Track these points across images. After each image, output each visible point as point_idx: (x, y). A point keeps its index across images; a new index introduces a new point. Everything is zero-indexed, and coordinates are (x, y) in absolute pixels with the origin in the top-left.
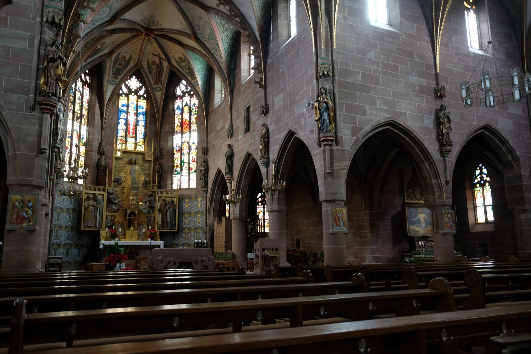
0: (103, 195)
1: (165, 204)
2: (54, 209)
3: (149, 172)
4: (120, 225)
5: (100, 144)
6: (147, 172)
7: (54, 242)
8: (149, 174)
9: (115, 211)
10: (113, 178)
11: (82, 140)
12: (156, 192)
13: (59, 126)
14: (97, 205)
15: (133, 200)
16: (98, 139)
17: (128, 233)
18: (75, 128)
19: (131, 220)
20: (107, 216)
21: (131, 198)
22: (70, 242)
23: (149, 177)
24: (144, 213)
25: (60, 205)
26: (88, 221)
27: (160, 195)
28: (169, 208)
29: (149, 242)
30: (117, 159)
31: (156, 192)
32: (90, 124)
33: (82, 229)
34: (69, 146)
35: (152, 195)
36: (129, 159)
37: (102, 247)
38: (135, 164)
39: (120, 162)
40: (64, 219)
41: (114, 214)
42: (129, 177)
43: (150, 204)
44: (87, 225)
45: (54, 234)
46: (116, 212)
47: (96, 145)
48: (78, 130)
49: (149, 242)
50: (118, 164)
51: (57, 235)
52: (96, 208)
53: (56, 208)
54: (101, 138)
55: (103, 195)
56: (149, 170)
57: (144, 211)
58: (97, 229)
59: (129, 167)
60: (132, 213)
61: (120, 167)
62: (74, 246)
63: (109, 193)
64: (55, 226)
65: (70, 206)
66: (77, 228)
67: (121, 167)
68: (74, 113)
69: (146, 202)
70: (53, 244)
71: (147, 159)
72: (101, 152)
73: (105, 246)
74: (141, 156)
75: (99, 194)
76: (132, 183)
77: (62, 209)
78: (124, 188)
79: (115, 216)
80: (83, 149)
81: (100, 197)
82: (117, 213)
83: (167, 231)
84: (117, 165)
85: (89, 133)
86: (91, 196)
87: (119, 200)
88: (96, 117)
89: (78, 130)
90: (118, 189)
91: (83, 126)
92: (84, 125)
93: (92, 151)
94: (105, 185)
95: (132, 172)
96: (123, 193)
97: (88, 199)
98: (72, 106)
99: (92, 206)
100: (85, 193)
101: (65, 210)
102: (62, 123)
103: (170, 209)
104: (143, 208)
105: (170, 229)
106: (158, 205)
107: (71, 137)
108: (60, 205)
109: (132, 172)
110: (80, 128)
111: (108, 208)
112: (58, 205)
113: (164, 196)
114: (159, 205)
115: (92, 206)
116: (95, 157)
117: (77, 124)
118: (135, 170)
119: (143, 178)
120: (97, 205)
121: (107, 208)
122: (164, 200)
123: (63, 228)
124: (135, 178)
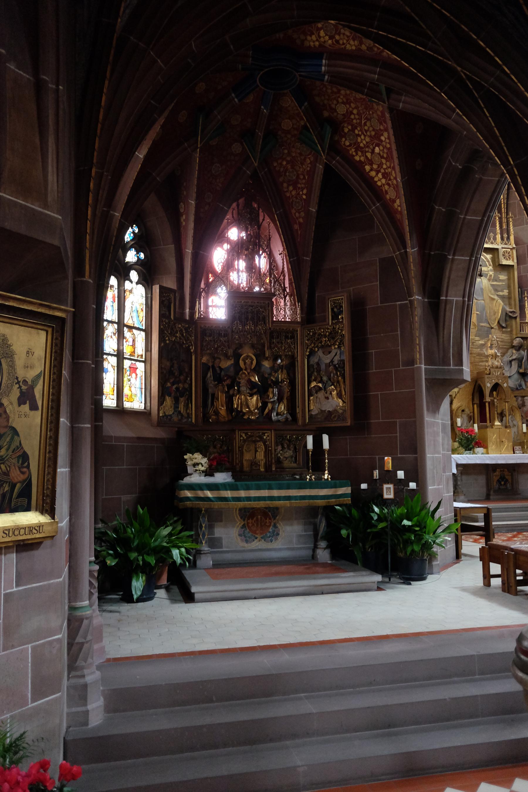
4: (465, 416)
6: (506, 292)
8: (509, 298)
17: (492, 435)
23: (510, 304)
43: (520, 366)
71: (505, 262)
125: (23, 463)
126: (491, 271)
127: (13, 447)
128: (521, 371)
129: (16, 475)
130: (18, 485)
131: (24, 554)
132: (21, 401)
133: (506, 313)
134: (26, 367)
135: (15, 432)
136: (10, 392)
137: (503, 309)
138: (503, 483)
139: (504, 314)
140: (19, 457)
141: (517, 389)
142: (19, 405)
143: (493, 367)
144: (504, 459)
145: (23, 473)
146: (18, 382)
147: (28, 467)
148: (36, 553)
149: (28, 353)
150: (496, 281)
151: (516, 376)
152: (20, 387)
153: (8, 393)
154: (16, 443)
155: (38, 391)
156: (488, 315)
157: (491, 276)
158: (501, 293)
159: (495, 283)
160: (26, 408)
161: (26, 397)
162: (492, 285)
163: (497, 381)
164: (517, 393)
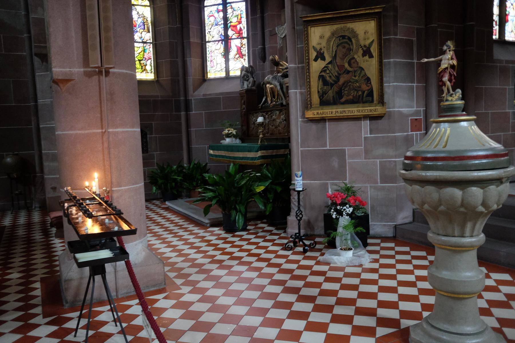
125: (368, 82)
127: (361, 75)
129: (364, 87)
130: (366, 92)
131: (373, 121)
132: (364, 55)
134: (365, 39)
135: (362, 69)
136: (357, 52)
140: (365, 79)
142: (363, 57)
145: (368, 86)
146: (361, 47)
147: (370, 83)
148: (380, 121)
149: (365, 33)
152: (363, 49)
153: (357, 52)
154: (363, 74)
160: (367, 57)
161: (367, 52)
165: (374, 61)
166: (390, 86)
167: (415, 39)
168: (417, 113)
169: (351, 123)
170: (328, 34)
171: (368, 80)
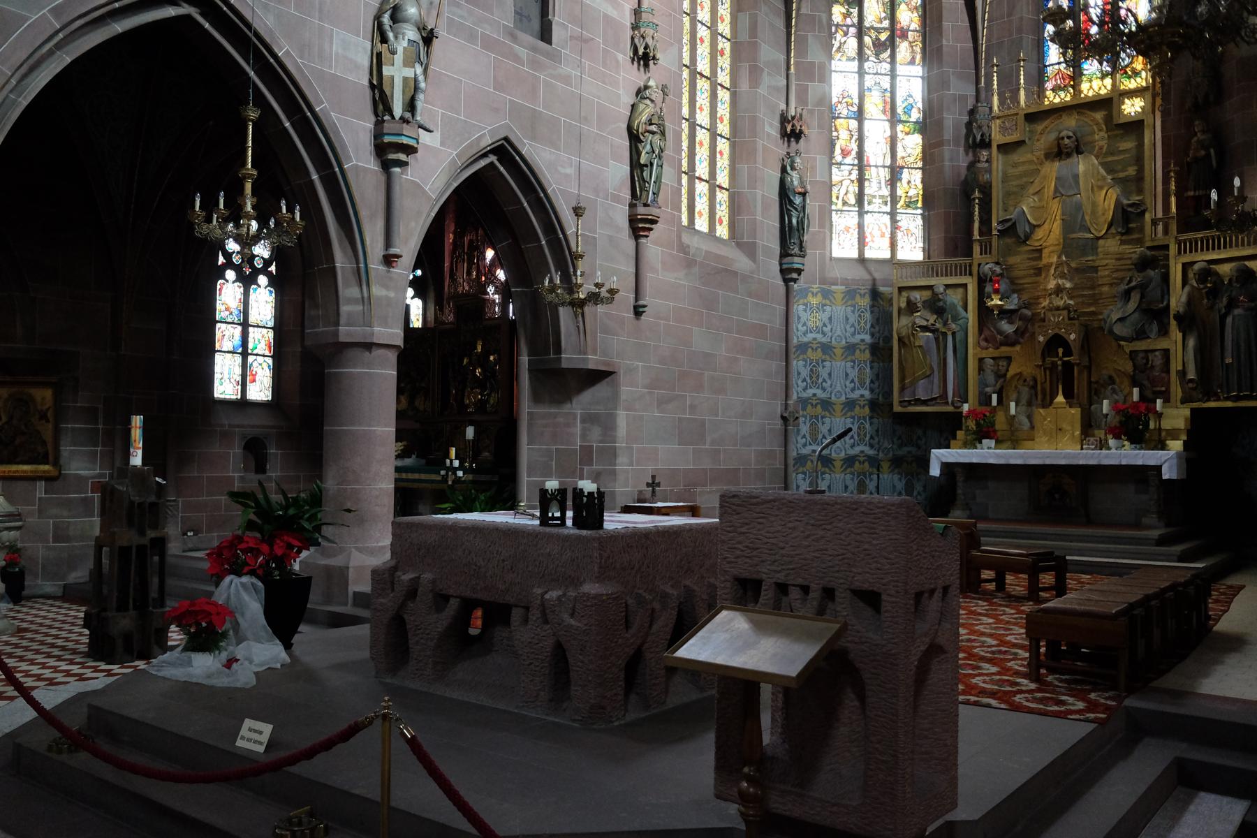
0: (965, 286)
1: (1214, 293)
2: (792, 356)
3: (1141, 170)
5: (972, 112)
6: (1131, 171)
7: (805, 451)
9: (1009, 341)
10: (994, 224)
11: (908, 111)
12: (1173, 249)
13: (386, 71)
14: (945, 324)
15: (1059, 290)
16: (963, 98)
18: (869, 81)
19: (1066, 367)
20: (981, 360)
21: (1052, 284)
22: (871, 452)
24: (1118, 338)
25: (819, 336)
26: (914, 383)
27: (1187, 258)
28: (1232, 304)
29: (1123, 454)
30: (1005, 148)
31: (1173, 249)
32: (931, 52)
33: (897, 408)
34: (854, 146)
35: (1154, 261)
36: (1053, 136)
37: (935, 471)
38: (1079, 152)
39: (1019, 156)
40: (845, 380)
41: (1005, 350)
42: (1055, 207)
43: (1141, 298)
44: (914, 393)
45: (804, 429)
46: (1013, 345)
47: (954, 119)
48: (886, 82)
49: (1123, 454)
50: (1015, 165)
51: (814, 431)
52: (940, 337)
53: (803, 347)
54: (977, 91)
55: (965, 286)
56: (1139, 160)
57: (1118, 329)
58: (950, 409)
59: (1053, 169)
60: (1057, 341)
61: (1020, 176)
62: (885, 466)
63: (982, 281)
64: (804, 402)
65: (858, 338)
66: (879, 406)
67: (1025, 174)
68: (861, 32)
69: (1127, 295)
70: (801, 460)
72: (977, 143)
73: (947, 467)
74: (1099, 116)
75: (947, 286)
76: (1068, 227)
77: (826, 348)
78: (1040, 251)
79: (1009, 359)
80: (912, 145)
81: (954, 297)
82: (1018, 348)
83: (1229, 404)
84: (1011, 171)
85: (933, 85)
86: (917, 296)
87: (1025, 297)
88: (946, 24)
89: (887, 86)
90: (1018, 260)
91: (900, 69)
92: (912, 62)
93: (940, 144)
94: (969, 253)
95: (1065, 187)
96: (1039, 271)
97: (911, 308)
98: (855, 12)
99: (925, 329)
100: (901, 289)
101: (838, 352)
102: (399, 58)
103: (1237, 311)
104: (1115, 317)
105: (1237, 398)
106: (1177, 299)
107: (860, 115)
108: (819, 336)
109: (1065, 187)
110: (893, 75)
111: (986, 333)
112: (810, 336)
113: (1202, 257)
114: (1184, 299)
115: (925, 329)
116: (956, 159)
117: (877, 66)
118: (1076, 177)
119: (1107, 200)
120: (945, 324)
121: (981, 331)
122: (1206, 274)
123: (838, 408)
124: (1079, 207)
126: (1103, 139)
128: (1144, 306)
133: (1124, 211)
137: (1118, 203)
138: (1057, 496)
139: (1120, 210)
141: (1137, 339)
143: (1051, 310)
144: (1021, 456)
150: (1112, 154)
151: (1136, 315)
155: (49, 414)
156: (1087, 218)
157: (1101, 148)
158: (1121, 175)
159: (1110, 159)
161: (43, 416)
162: (1103, 164)
163: (1056, 331)
164: (1141, 345)
165: (50, 426)
166: (66, 449)
167: (101, 406)
168: (101, 476)
169: (26, 484)
170: (5, 395)
171: (44, 443)
